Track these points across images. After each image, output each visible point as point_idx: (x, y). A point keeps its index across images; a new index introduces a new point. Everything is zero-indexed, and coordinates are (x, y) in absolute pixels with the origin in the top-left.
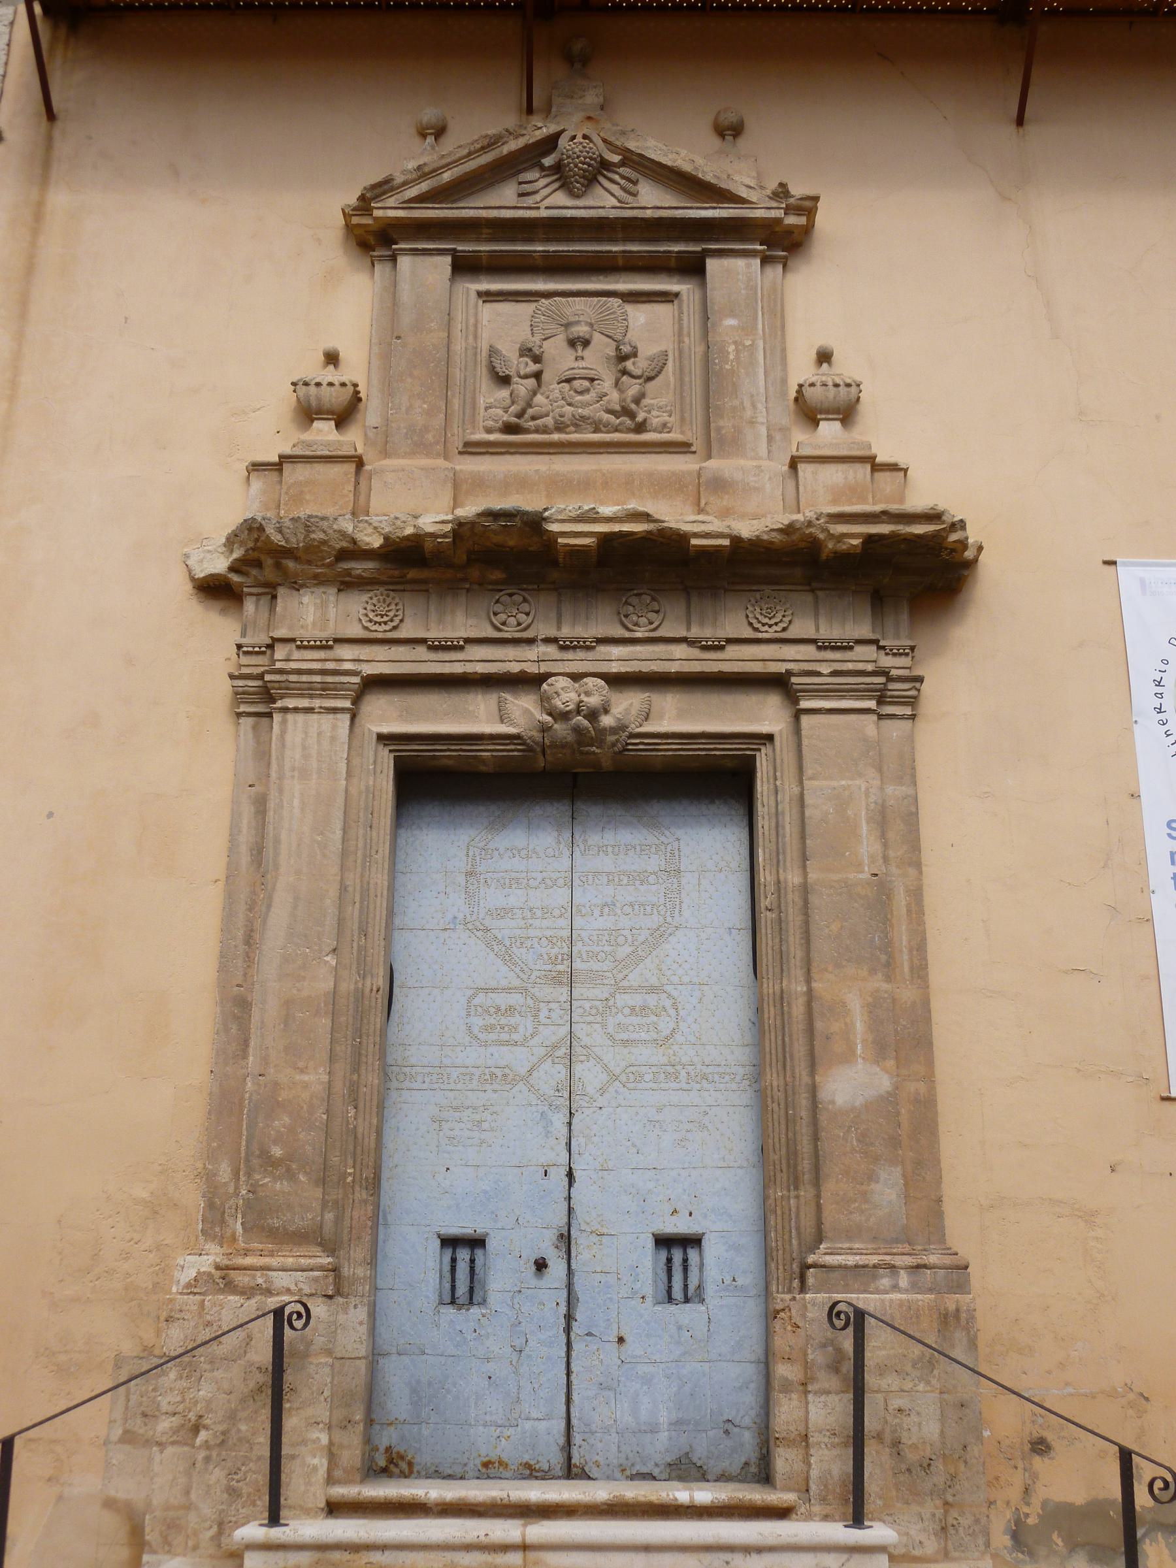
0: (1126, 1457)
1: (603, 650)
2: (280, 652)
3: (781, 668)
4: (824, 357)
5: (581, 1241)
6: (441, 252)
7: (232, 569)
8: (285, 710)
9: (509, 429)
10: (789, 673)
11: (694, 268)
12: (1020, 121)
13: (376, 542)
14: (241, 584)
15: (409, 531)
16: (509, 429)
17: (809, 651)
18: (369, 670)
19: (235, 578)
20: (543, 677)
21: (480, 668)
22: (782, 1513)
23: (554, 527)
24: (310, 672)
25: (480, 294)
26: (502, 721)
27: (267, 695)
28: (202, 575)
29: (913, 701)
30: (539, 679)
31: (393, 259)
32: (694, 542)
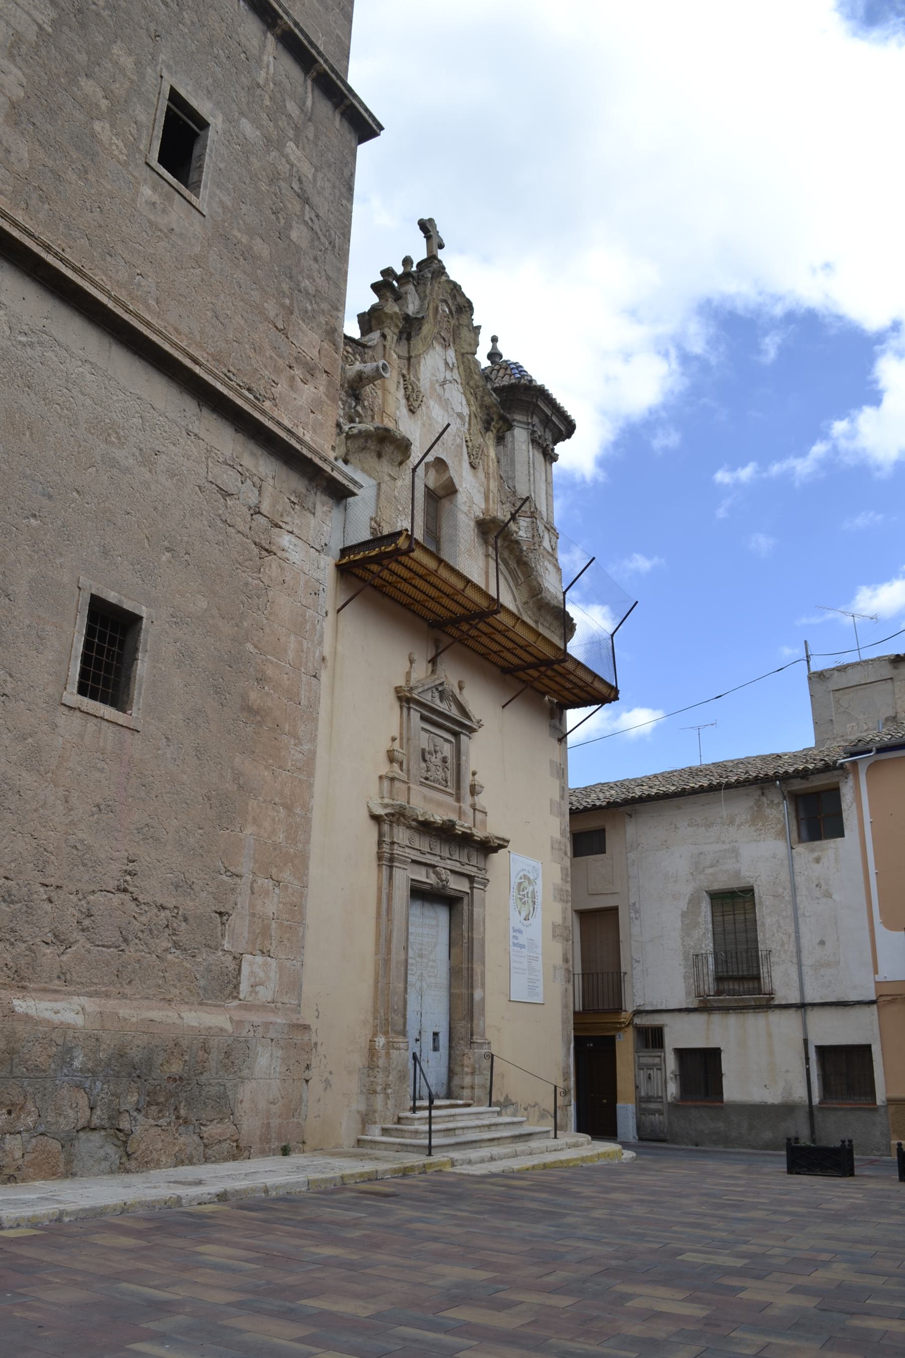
0: (555, 1087)
1: (447, 860)
2: (396, 846)
3: (473, 874)
4: (474, 774)
5: (423, 1033)
6: (419, 711)
7: (386, 815)
8: (396, 867)
9: (427, 779)
10: (475, 876)
11: (456, 734)
12: (503, 707)
13: (421, 818)
14: (385, 820)
15: (432, 820)
16: (427, 779)
17: (475, 869)
18: (414, 858)
19: (386, 818)
20: (437, 866)
21: (428, 862)
22: (469, 1105)
23: (457, 827)
24: (402, 856)
25: (422, 728)
26: (427, 878)
27: (392, 859)
28: (377, 813)
29: (485, 885)
30: (434, 866)
31: (409, 709)
32: (476, 838)
